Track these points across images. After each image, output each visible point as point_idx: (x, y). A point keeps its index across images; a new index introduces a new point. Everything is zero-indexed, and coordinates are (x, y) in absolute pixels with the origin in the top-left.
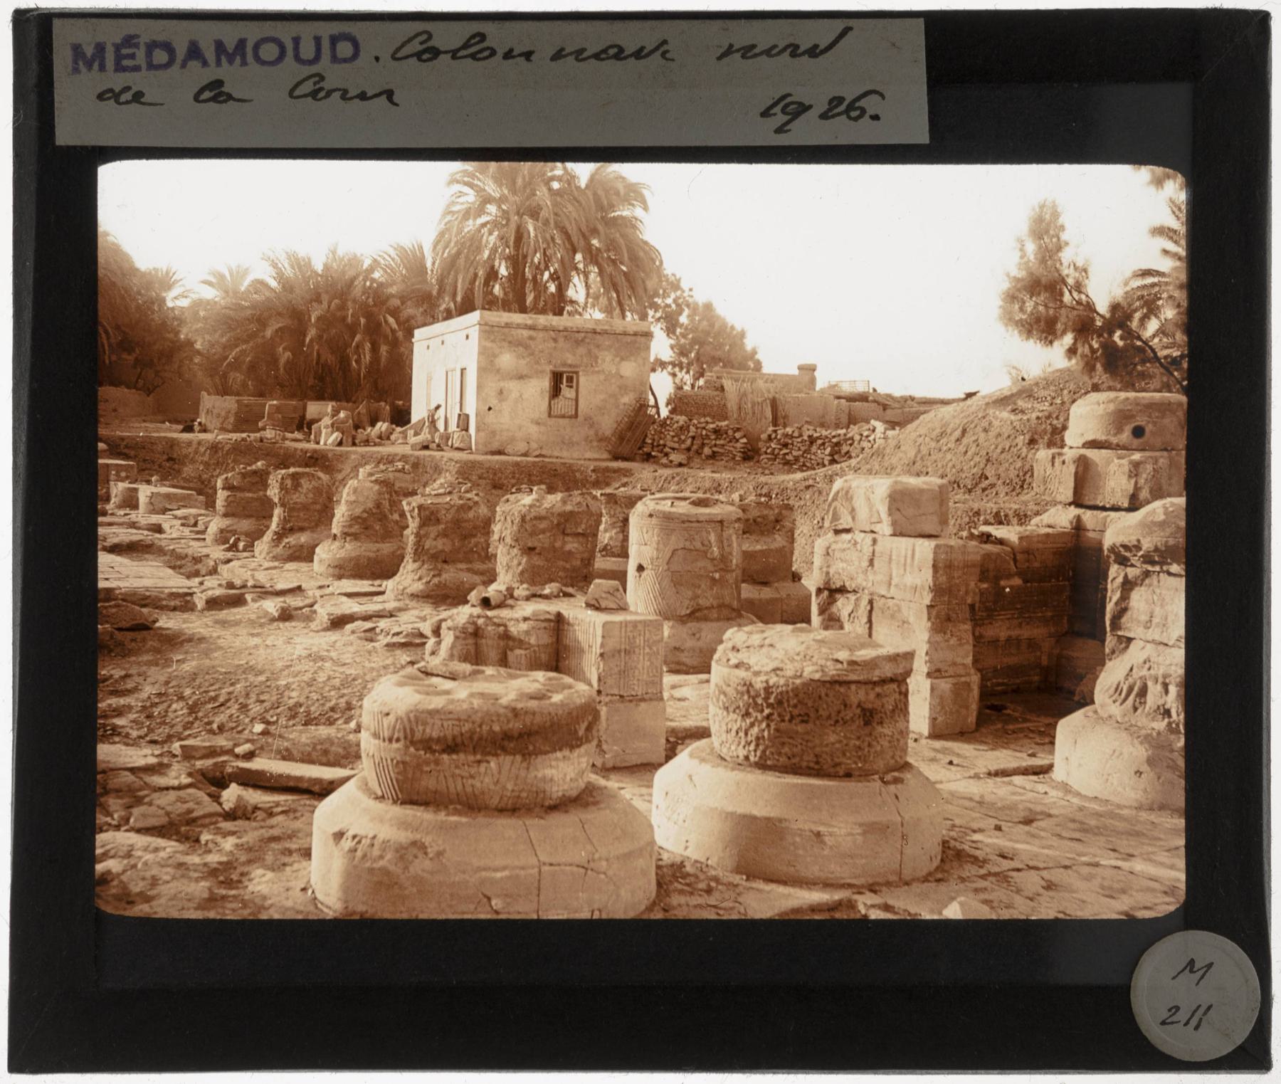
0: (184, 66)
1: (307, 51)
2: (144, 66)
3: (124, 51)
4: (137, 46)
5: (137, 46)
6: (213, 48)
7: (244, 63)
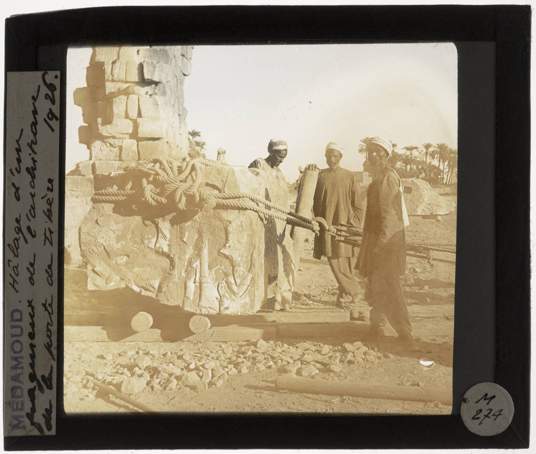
0: (22, 383)
2: (22, 399)
3: (15, 408)
4: (13, 402)
7: (22, 358)
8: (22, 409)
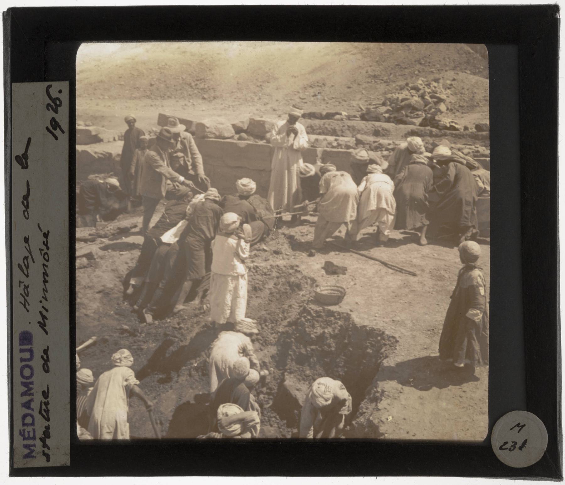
0: (33, 410)
1: (27, 355)
2: (34, 427)
3: (27, 436)
4: (24, 430)
5: (24, 430)
6: (24, 397)
7: (32, 383)
8: (34, 438)
